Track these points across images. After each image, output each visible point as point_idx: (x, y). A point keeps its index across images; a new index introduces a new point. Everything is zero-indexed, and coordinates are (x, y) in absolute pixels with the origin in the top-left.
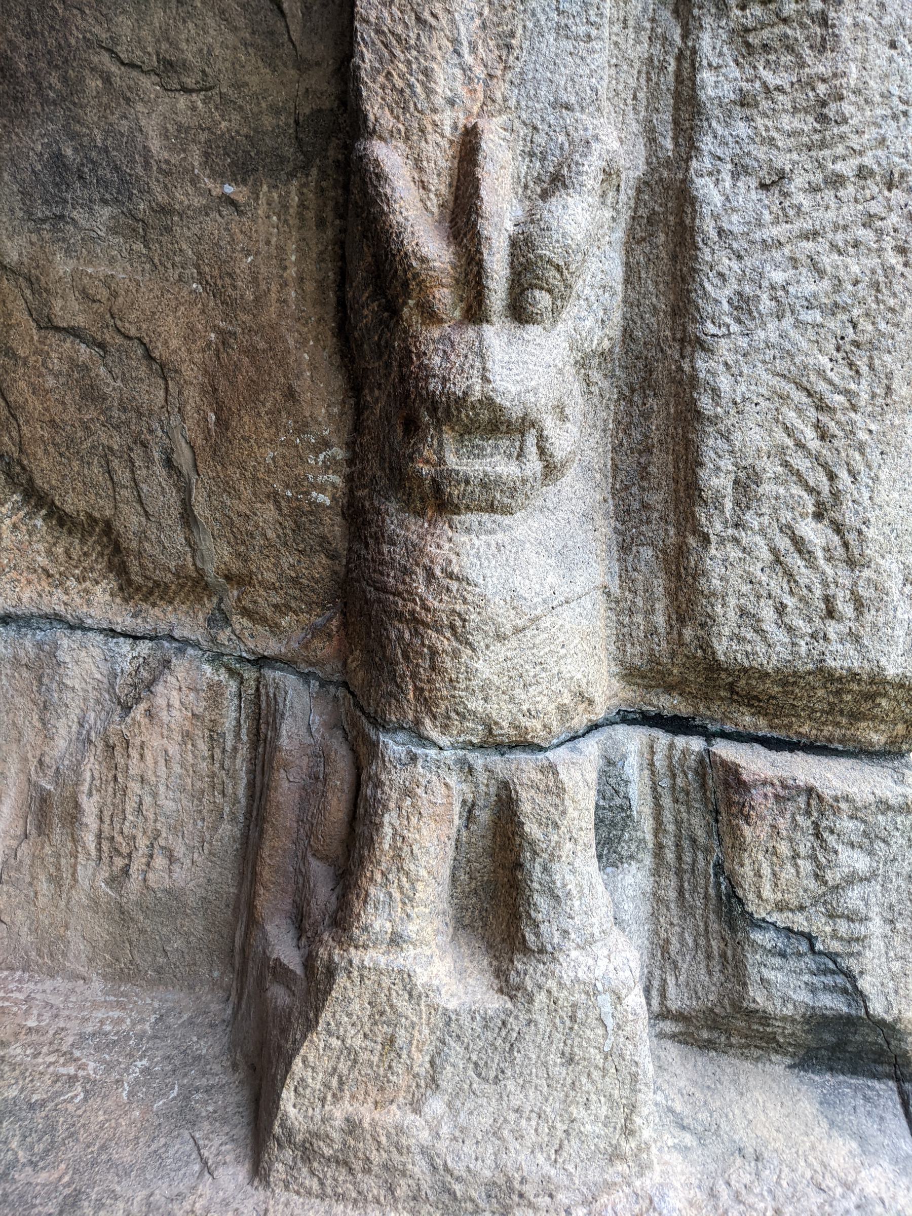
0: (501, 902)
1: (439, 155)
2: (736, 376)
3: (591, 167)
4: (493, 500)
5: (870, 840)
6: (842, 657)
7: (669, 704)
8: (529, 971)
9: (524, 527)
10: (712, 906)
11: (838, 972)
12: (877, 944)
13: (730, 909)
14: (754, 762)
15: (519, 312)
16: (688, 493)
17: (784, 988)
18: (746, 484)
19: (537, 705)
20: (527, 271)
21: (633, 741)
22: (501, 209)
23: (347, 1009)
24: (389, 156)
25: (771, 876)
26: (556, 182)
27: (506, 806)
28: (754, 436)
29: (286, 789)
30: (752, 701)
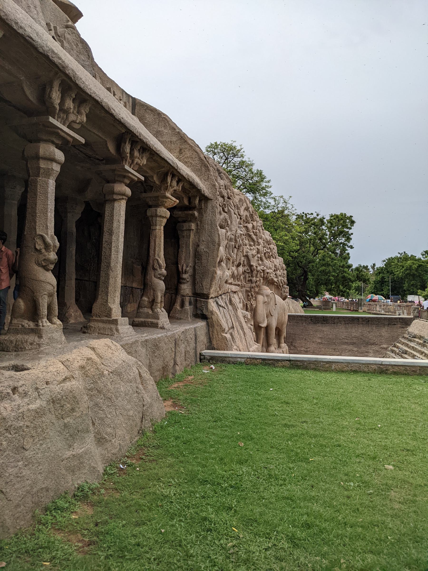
0: (182, 305)
1: (182, 265)
2: (197, 277)
3: (189, 266)
4: (184, 283)
5: (204, 303)
6: (202, 292)
7: (195, 296)
8: (183, 308)
9: (186, 285)
10: (196, 307)
11: (202, 311)
12: (204, 310)
13: (197, 308)
14: (198, 299)
15: (185, 273)
16: (195, 283)
17: (199, 312)
18: (198, 282)
19: (185, 294)
20: (185, 272)
21: (192, 298)
22: (184, 268)
23: (174, 309)
24: (179, 265)
25: (198, 305)
26: (187, 267)
27: (183, 300)
28: (198, 280)
29: (172, 301)
30: (199, 296)
